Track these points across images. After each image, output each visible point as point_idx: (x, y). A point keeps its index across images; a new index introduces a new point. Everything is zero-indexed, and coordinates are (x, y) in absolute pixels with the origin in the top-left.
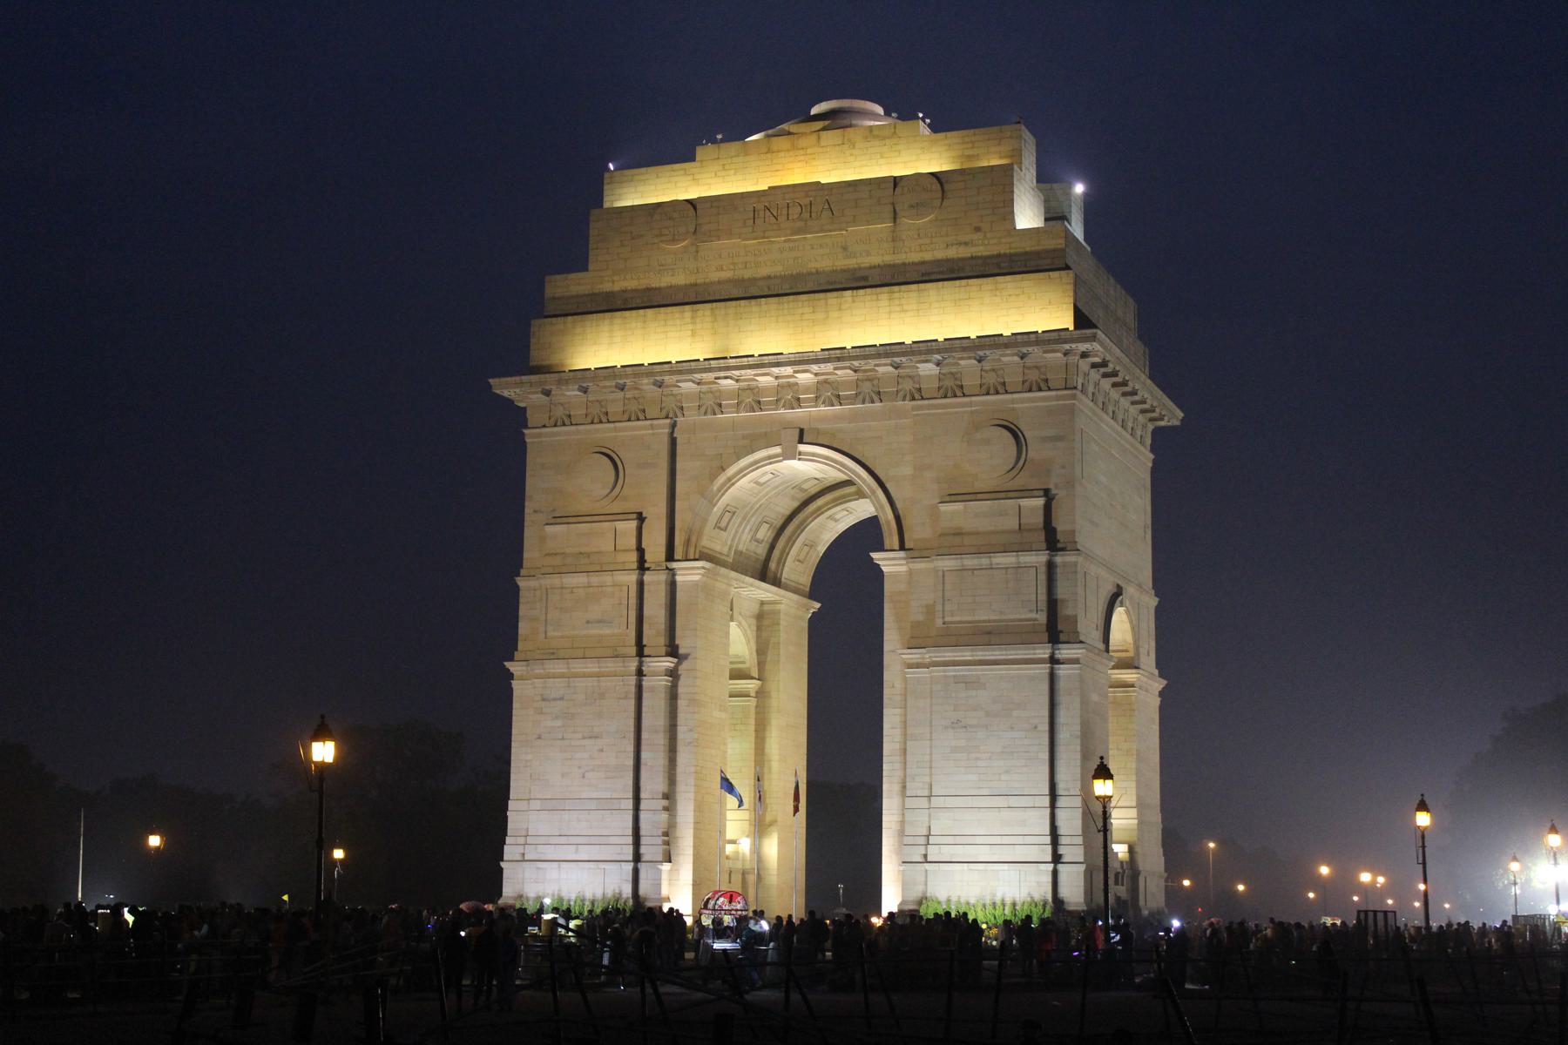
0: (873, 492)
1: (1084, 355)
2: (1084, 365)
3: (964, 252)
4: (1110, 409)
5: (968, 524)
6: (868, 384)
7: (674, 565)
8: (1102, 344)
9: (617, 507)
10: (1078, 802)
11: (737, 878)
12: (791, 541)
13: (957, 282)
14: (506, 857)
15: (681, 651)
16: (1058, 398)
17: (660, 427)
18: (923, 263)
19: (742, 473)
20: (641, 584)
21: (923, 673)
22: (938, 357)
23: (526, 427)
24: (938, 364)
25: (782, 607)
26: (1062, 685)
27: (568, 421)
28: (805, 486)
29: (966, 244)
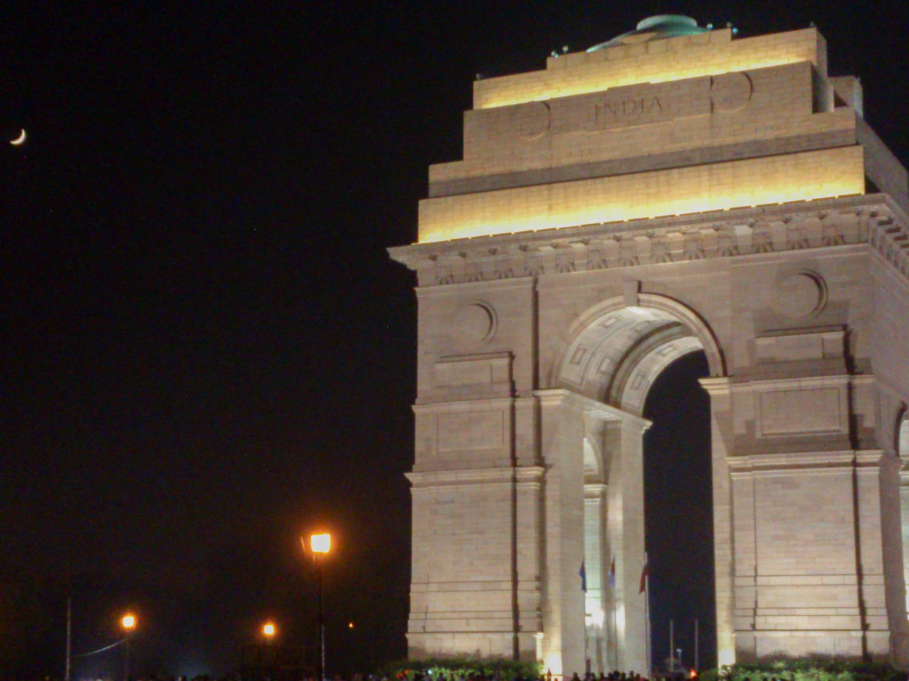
0: (700, 331)
1: (873, 215)
2: (873, 223)
3: (770, 135)
4: (893, 258)
5: (779, 355)
7: (540, 393)
8: (888, 205)
9: (492, 348)
10: (881, 580)
11: (592, 645)
12: (628, 372)
13: (765, 160)
14: (410, 629)
18: (736, 145)
19: (594, 317)
20: (513, 409)
21: (747, 476)
24: (751, 226)
25: (623, 426)
26: (862, 484)
27: (450, 279)
28: (639, 328)
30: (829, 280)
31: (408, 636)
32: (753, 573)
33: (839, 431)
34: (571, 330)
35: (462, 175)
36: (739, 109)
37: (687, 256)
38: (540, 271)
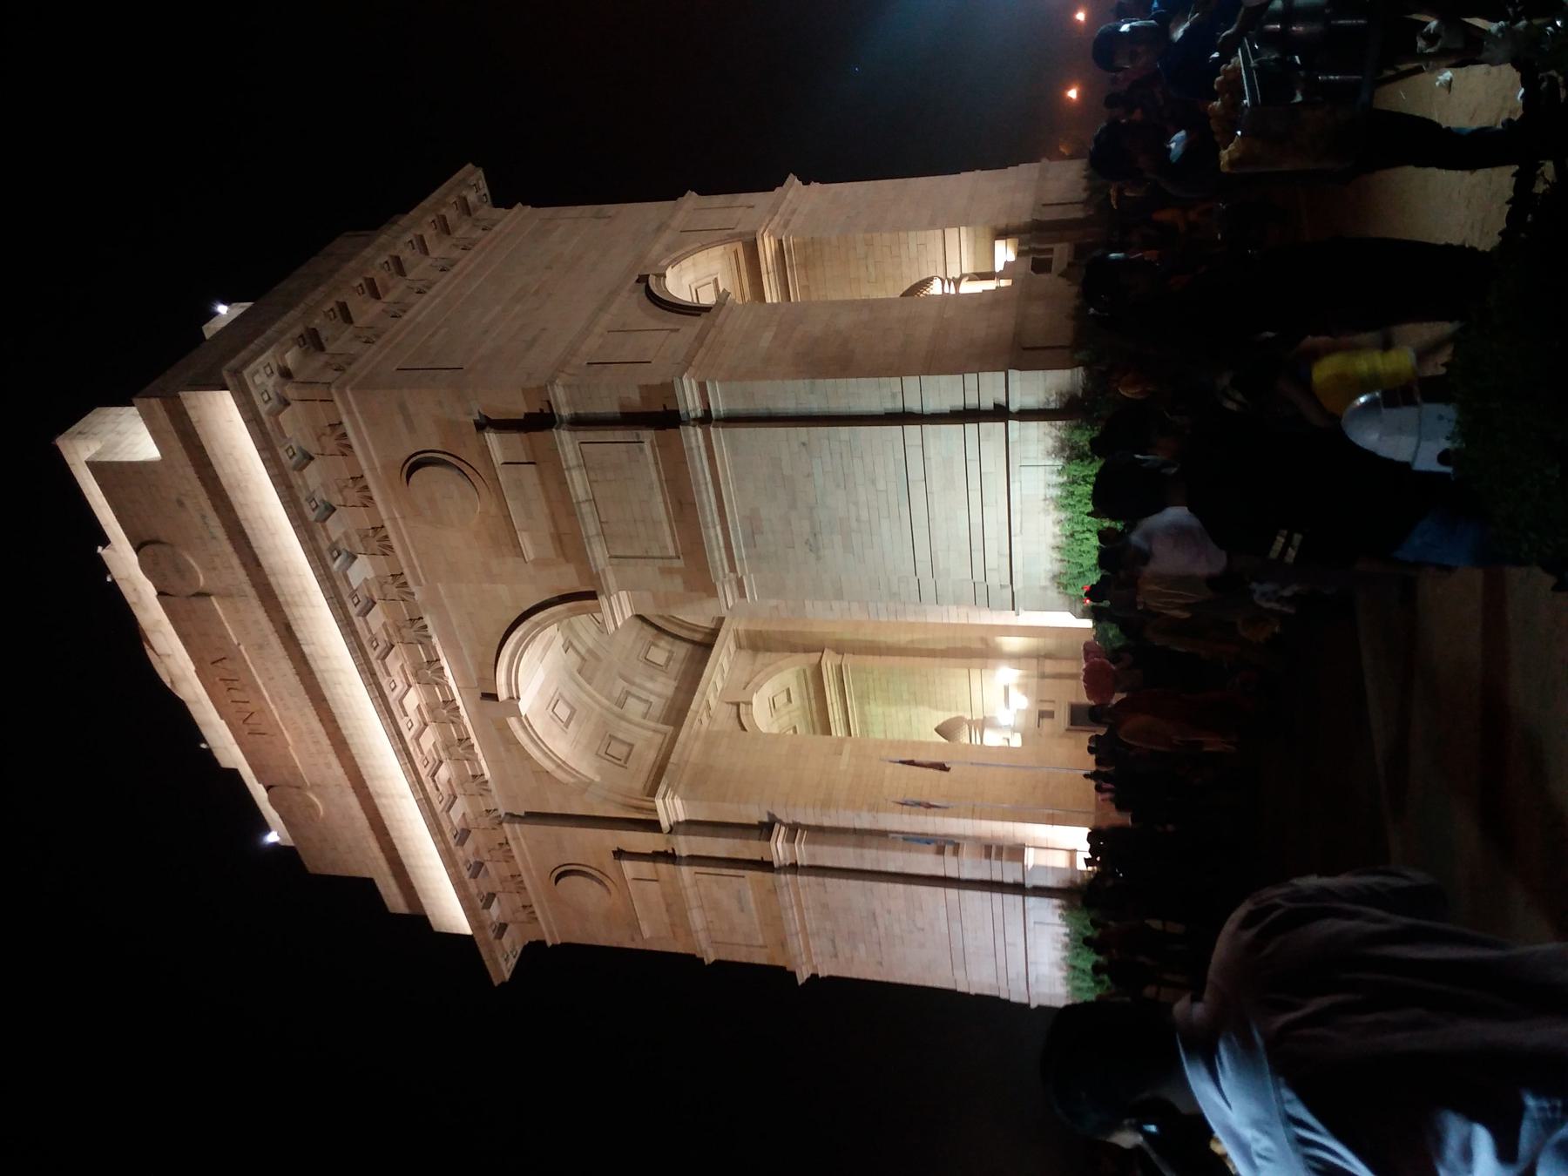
3: (214, 521)
6: (404, 631)
7: (665, 824)
10: (911, 382)
14: (1025, 1001)
15: (766, 819)
16: (350, 412)
17: (514, 832)
19: (548, 754)
22: (335, 566)
23: (544, 942)
24: (353, 557)
25: (741, 628)
26: (741, 406)
29: (204, 517)
30: (409, 447)
31: (1033, 1005)
35: (392, 882)
36: (192, 561)
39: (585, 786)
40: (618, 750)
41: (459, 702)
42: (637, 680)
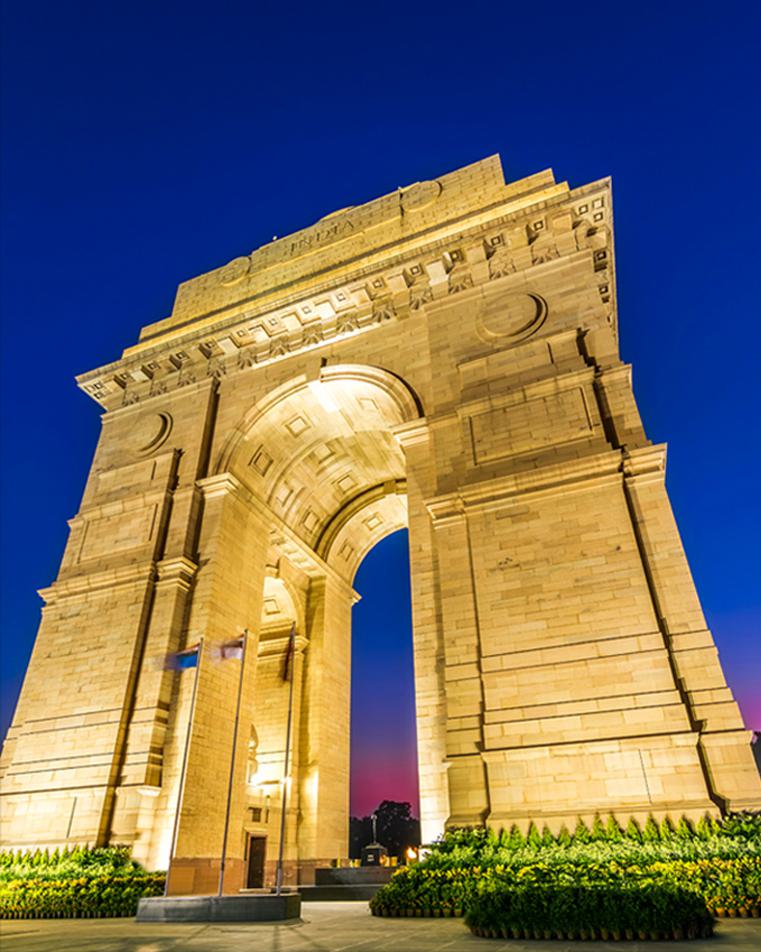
3: (462, 213)
6: (384, 306)
7: (203, 482)
15: (202, 558)
17: (206, 385)
21: (458, 521)
25: (327, 582)
32: (474, 657)
33: (587, 437)
34: (247, 421)
37: (376, 318)
38: (221, 373)
39: (240, 427)
40: (263, 463)
41: (321, 343)
42: (299, 501)
